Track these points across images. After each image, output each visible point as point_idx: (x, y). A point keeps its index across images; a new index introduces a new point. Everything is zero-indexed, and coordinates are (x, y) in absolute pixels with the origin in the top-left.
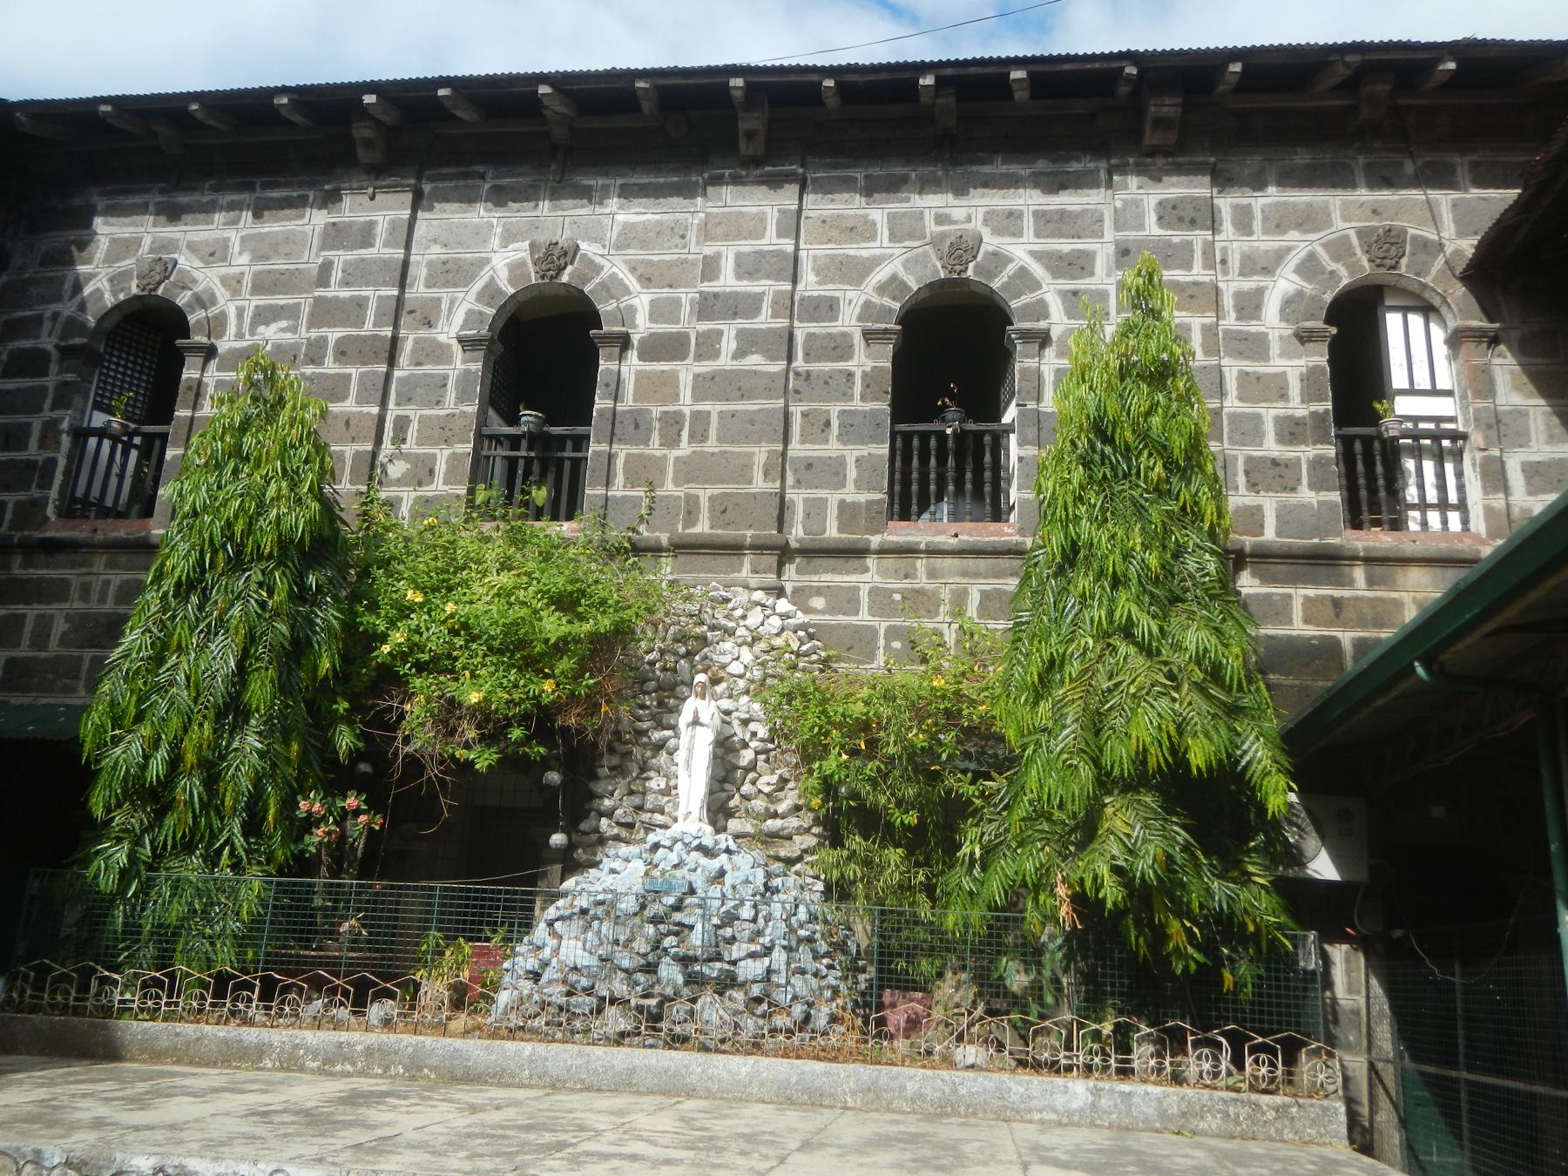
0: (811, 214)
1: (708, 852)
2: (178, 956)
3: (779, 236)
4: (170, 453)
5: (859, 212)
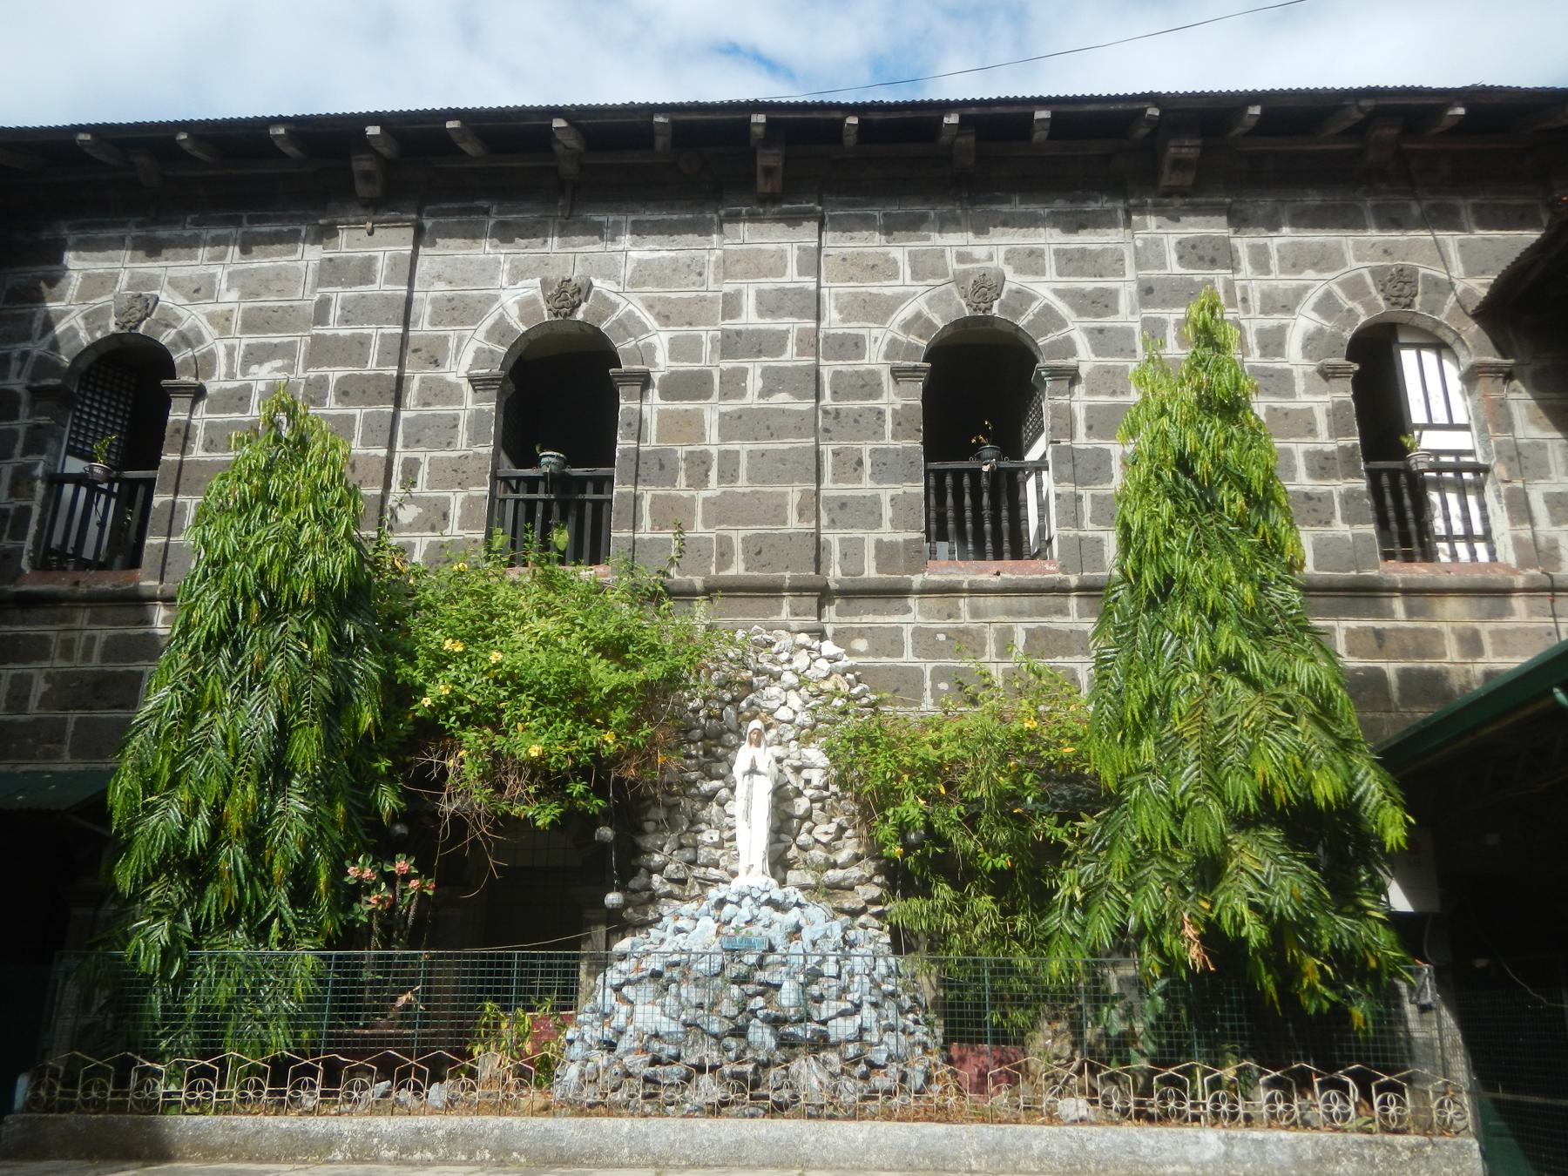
0: (830, 251)
2: (229, 1040)
3: (800, 274)
4: (157, 500)
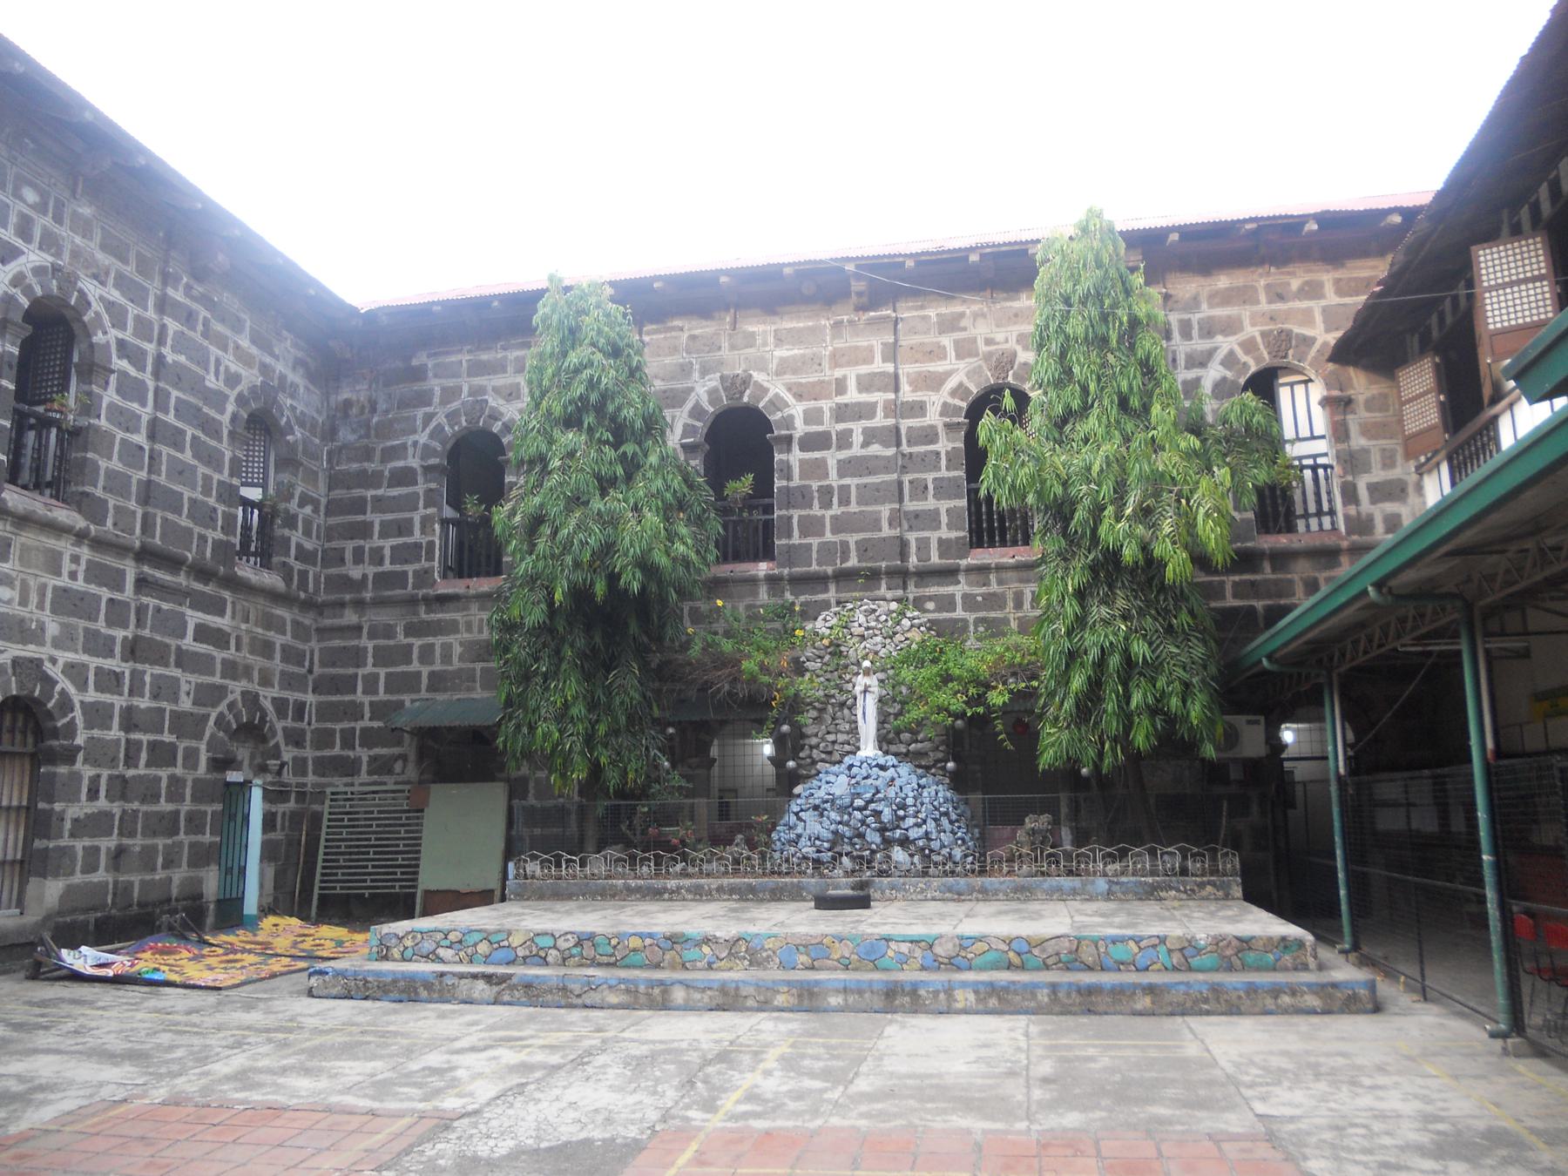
1: (883, 768)
5: (935, 340)
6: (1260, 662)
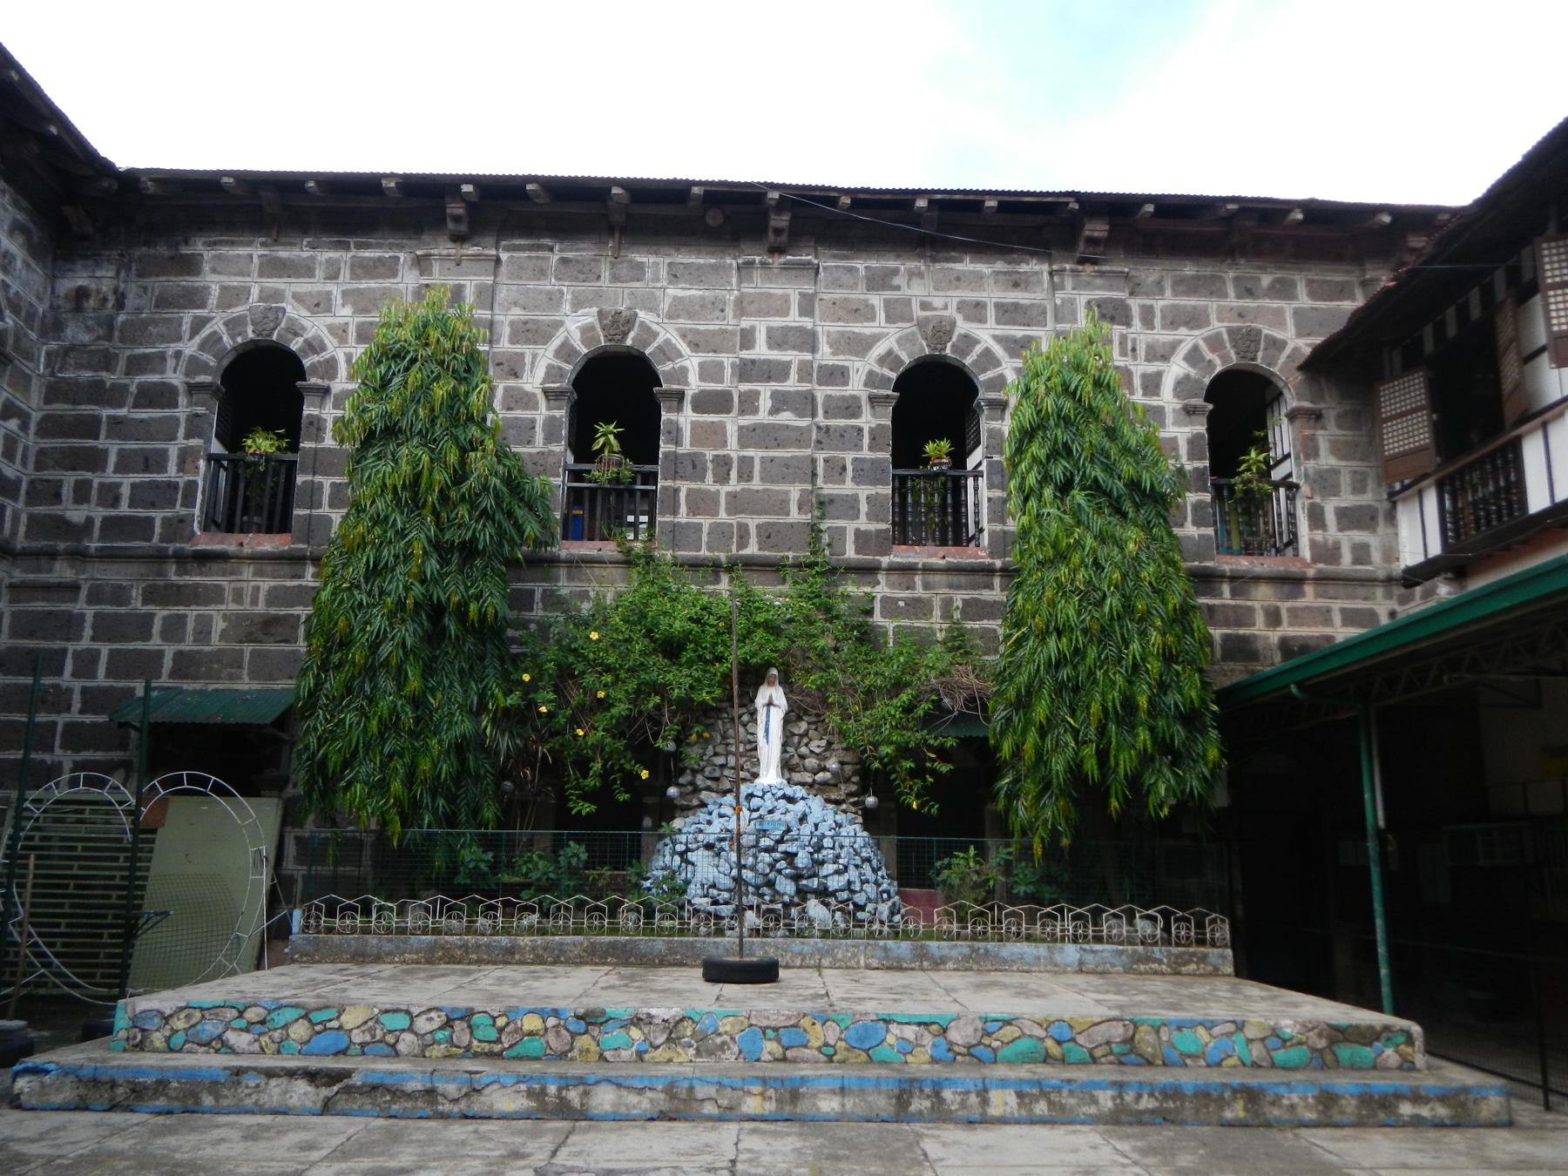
3: (800, 315)
5: (861, 297)
6: (1288, 686)
